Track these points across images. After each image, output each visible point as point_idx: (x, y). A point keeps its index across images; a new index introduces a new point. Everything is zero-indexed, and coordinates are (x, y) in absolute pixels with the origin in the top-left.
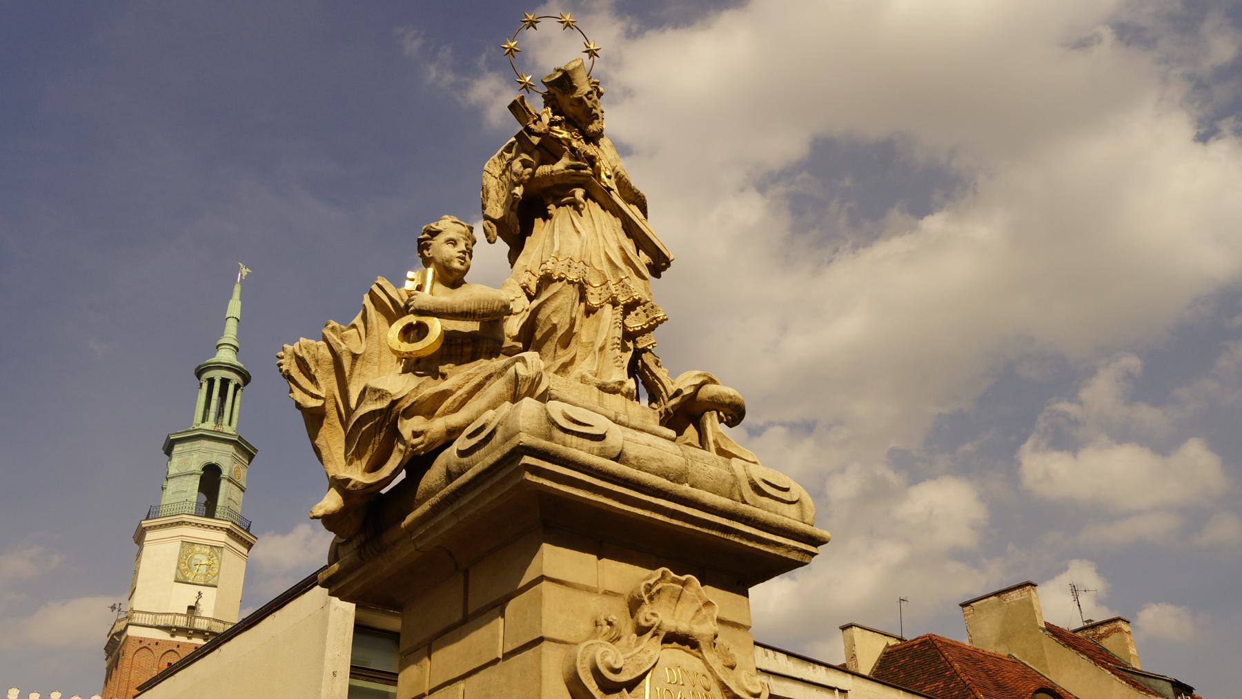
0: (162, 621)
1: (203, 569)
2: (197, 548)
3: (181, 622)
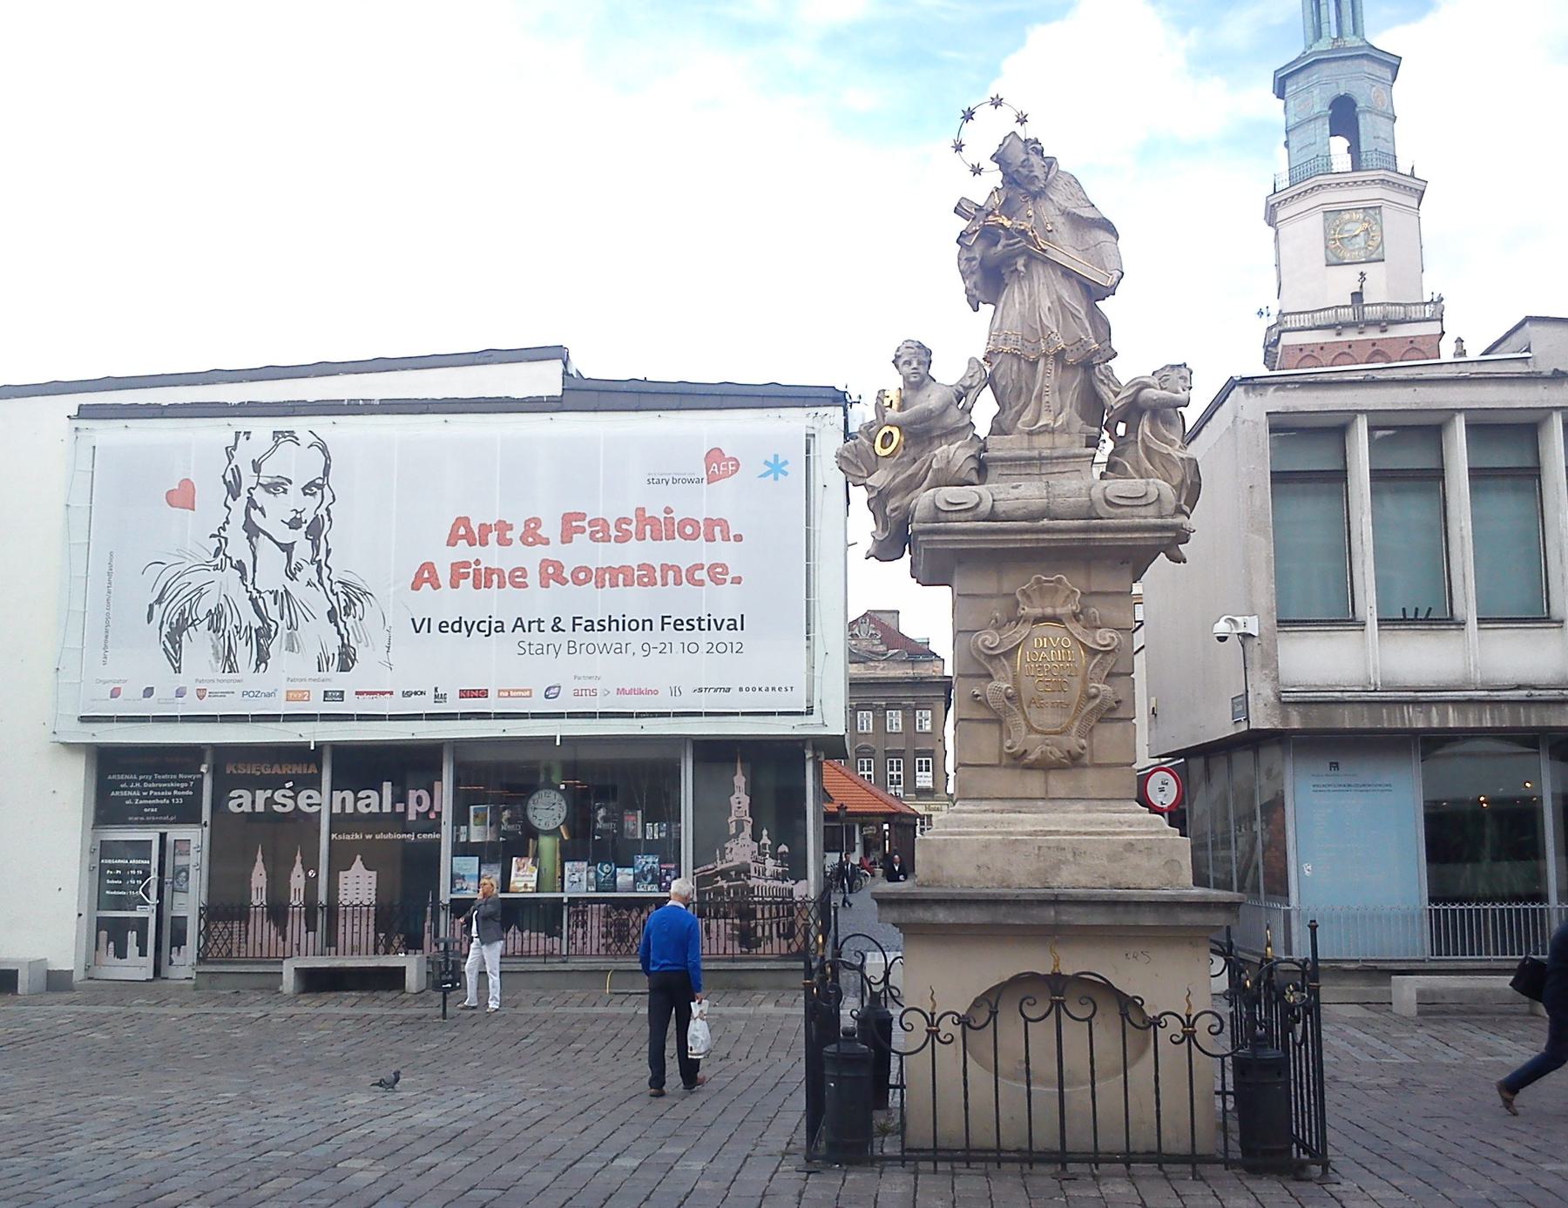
0: (1320, 318)
1: (1360, 241)
2: (1347, 216)
3: (1347, 315)
